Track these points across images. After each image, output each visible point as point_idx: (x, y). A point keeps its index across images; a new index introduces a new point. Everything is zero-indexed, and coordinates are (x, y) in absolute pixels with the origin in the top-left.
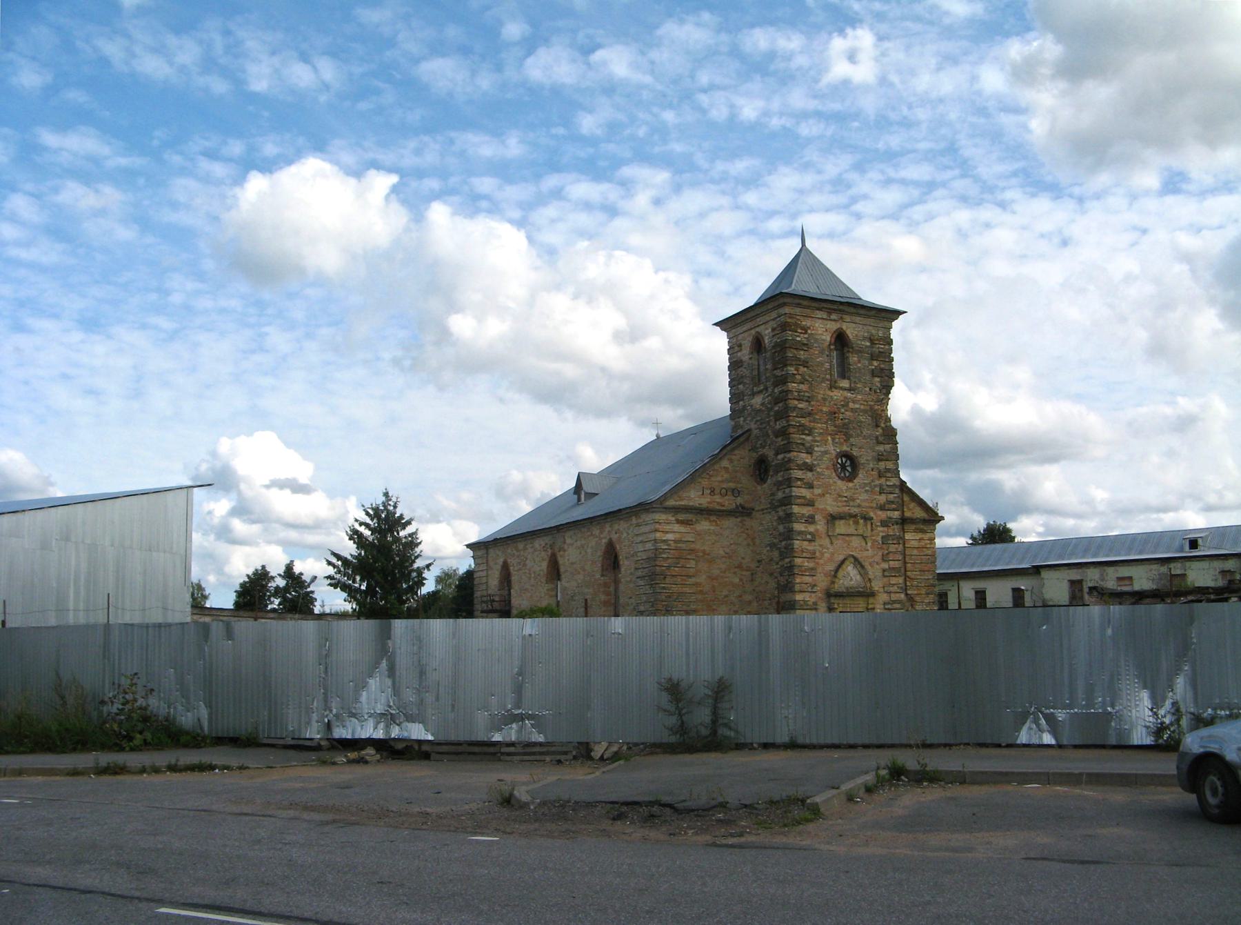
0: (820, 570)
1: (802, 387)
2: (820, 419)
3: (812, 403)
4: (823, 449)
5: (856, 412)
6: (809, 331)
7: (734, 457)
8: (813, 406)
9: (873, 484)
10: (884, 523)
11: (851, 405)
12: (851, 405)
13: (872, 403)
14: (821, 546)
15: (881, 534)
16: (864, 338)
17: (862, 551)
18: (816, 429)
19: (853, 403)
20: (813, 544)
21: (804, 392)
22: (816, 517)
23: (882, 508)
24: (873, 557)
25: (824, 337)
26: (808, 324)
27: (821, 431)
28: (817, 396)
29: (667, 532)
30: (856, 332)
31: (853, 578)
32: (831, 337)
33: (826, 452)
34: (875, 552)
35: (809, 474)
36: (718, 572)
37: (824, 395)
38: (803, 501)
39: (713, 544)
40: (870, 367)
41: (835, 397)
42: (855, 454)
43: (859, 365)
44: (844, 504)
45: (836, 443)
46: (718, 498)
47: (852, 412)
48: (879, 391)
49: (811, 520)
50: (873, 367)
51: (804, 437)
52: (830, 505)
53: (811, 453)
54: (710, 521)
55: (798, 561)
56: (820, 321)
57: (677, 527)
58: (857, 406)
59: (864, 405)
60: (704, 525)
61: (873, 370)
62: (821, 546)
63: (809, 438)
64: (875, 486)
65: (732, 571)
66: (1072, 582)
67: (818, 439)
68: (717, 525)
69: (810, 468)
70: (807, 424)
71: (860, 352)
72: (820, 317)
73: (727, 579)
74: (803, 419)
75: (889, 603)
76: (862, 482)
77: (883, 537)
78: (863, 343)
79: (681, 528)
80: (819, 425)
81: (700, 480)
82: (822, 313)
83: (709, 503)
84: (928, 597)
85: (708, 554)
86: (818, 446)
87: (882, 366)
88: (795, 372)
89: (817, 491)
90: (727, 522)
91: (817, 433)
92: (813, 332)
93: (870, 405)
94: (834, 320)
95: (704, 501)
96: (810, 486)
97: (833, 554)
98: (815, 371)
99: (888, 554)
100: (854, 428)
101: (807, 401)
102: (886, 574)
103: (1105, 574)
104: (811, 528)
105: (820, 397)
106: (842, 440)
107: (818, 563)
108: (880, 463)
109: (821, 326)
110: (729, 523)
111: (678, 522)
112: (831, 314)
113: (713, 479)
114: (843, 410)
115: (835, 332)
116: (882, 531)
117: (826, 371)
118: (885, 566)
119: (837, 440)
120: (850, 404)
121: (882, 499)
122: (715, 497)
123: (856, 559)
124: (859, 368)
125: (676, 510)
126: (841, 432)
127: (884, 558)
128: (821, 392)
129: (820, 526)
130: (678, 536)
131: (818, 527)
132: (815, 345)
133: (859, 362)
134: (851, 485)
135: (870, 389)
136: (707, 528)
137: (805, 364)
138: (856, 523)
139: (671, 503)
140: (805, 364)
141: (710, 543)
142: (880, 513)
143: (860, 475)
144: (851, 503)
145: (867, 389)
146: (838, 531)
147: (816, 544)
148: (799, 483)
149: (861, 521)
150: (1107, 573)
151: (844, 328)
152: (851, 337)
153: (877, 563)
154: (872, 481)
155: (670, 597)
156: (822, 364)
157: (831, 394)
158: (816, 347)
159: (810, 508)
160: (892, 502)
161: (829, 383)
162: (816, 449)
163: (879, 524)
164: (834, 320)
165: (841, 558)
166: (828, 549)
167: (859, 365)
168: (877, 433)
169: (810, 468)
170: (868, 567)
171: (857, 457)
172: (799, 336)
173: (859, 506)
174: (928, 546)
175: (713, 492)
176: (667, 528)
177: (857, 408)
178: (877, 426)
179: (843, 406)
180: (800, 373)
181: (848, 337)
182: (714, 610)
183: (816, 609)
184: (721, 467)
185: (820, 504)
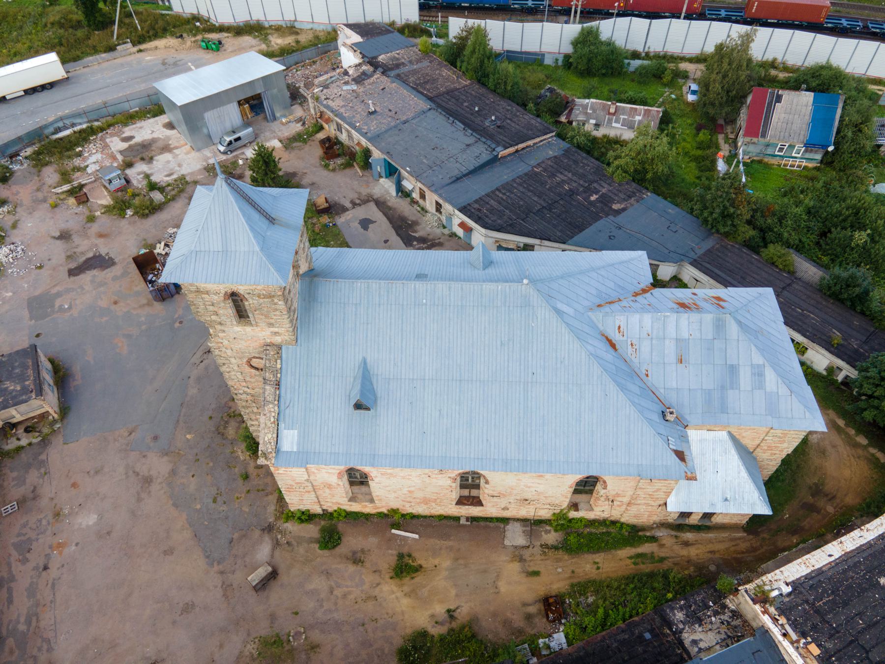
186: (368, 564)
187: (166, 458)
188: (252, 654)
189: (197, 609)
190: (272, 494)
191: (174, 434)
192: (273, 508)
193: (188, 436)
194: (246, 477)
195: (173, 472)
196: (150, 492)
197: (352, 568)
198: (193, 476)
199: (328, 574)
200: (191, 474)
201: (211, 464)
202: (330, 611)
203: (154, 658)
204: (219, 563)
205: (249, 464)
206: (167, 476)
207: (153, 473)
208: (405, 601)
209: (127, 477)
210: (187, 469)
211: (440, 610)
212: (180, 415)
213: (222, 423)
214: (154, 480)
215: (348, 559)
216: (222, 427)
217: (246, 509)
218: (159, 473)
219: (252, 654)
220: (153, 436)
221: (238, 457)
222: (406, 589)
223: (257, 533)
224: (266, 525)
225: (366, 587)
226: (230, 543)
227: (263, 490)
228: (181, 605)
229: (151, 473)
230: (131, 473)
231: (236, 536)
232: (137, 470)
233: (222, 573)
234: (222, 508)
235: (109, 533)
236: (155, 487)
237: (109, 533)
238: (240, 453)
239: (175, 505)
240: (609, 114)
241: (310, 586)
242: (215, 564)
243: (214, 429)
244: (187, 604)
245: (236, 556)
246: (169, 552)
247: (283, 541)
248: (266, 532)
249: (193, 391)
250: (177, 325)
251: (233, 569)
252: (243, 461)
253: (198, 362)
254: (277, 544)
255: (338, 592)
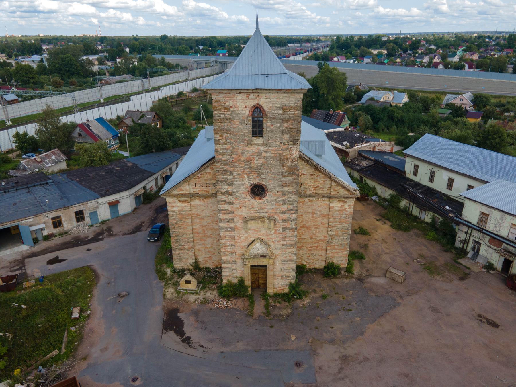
0: (238, 245)
1: (225, 146)
2: (239, 165)
3: (233, 156)
4: (240, 183)
5: (267, 158)
6: (232, 109)
7: (214, 167)
8: (233, 158)
9: (278, 200)
10: (284, 221)
11: (264, 154)
12: (264, 154)
13: (281, 152)
14: (238, 233)
15: (282, 227)
16: (278, 108)
17: (267, 235)
18: (236, 171)
19: (265, 152)
20: (233, 233)
21: (227, 149)
22: (235, 219)
23: (284, 213)
24: (274, 238)
25: (244, 112)
26: (231, 105)
27: (240, 172)
28: (237, 152)
29: (174, 207)
30: (271, 105)
31: (260, 249)
32: (250, 111)
33: (243, 184)
34: (277, 236)
35: (230, 197)
36: (206, 223)
37: (242, 150)
38: (226, 212)
39: (202, 211)
40: (281, 128)
41: (251, 151)
42: (265, 184)
43: (272, 128)
44: (256, 212)
45: (251, 179)
46: (204, 188)
47: (265, 159)
48: (286, 144)
49: (232, 220)
50: (284, 128)
51: (226, 177)
52: (245, 212)
53: (232, 186)
54: (200, 200)
55: (223, 241)
56: (241, 101)
57: (179, 204)
58: (268, 155)
59: (274, 153)
60: (196, 202)
61: (283, 130)
62: (238, 233)
63: (231, 177)
64: (279, 201)
65: (214, 223)
66: (483, 213)
67: (236, 177)
68: (205, 202)
69: (231, 194)
70: (229, 169)
71: (274, 118)
72: (241, 98)
73: (211, 227)
74: (225, 166)
75: (284, 261)
76: (270, 199)
77: (283, 228)
78: (276, 112)
79: (182, 204)
80: (238, 169)
81: (193, 180)
82: (241, 95)
83: (199, 191)
84: (343, 235)
85: (200, 216)
86: (236, 181)
87: (291, 126)
88: (221, 138)
89: (235, 206)
90: (210, 200)
91: (236, 174)
92: (234, 109)
93: (280, 154)
94: (252, 99)
95: (197, 190)
96: (231, 203)
97: (246, 238)
98: (236, 135)
99: (286, 237)
100: (265, 168)
101: (229, 155)
102: (283, 247)
103: (504, 218)
104: (232, 225)
105: (239, 151)
106: (255, 176)
107: (236, 242)
108: (284, 188)
109: (241, 104)
110: (210, 200)
111: (180, 201)
112: (249, 95)
113: (201, 179)
114: (257, 158)
115: (252, 107)
116: (282, 225)
117: (244, 134)
118: (285, 243)
119: (251, 177)
120: (263, 154)
121: (285, 207)
122: (203, 188)
123: (262, 240)
124: (272, 130)
125: (177, 196)
126: (255, 171)
127: (284, 238)
128: (240, 149)
129: (239, 223)
130: (180, 208)
131: (237, 224)
132: (236, 118)
133: (272, 125)
134: (261, 201)
135: (281, 143)
136: (199, 203)
137: (228, 131)
138: (263, 222)
139: (175, 192)
140: (228, 131)
141: (201, 210)
142: (282, 215)
143: (268, 196)
144: (261, 211)
145: (278, 143)
146: (249, 226)
147: (236, 233)
148: (223, 202)
149: (267, 221)
150: (506, 218)
151: (261, 103)
152: (266, 109)
153: (278, 241)
154: (277, 198)
155: (178, 235)
156: (241, 130)
157: (247, 148)
158: (237, 119)
159: (232, 215)
160: (292, 210)
161: (246, 142)
162: (235, 183)
163: (281, 221)
164: (252, 99)
165: (253, 239)
166: (244, 235)
167: (272, 128)
168: (284, 170)
169: (231, 194)
170: (272, 245)
171: (266, 186)
172: (223, 114)
173: (267, 212)
174: (348, 209)
175: (201, 185)
176: (174, 204)
177: (268, 156)
178: (283, 166)
179: (257, 156)
180: (224, 138)
181: (264, 109)
182: (204, 240)
183: (236, 264)
184: (206, 173)
185: (238, 213)
186: (366, 243)
187: (319, 351)
188: (441, 277)
189: (432, 305)
190: (335, 282)
191: (292, 350)
192: (345, 280)
193: (293, 338)
194: (324, 297)
195: (332, 342)
196: (356, 354)
197: (371, 247)
198: (332, 328)
199: (379, 255)
200: (330, 329)
201: (318, 318)
202: (399, 252)
203: (477, 321)
204: (396, 300)
205: (312, 297)
206: (336, 346)
207: (336, 356)
208: (380, 231)
209: (347, 377)
210: (326, 333)
211: (378, 223)
212: (270, 350)
213: (276, 318)
214: (344, 354)
215: (366, 249)
216: (281, 318)
217: (351, 292)
218: (335, 352)
219: (441, 277)
220: (295, 368)
221: (308, 303)
222: (373, 231)
223: (366, 285)
224: (359, 281)
225: (379, 243)
226: (379, 296)
227: (333, 286)
228: (434, 314)
229: (337, 358)
230: (341, 375)
231: (372, 294)
232: (336, 370)
233: (401, 297)
234: (355, 305)
235: (407, 375)
236: (350, 351)
237: (407, 375)
238: (305, 303)
239: (362, 333)
240: (39, 162)
241: (390, 261)
242: (397, 302)
243: (283, 323)
244: (432, 311)
245: (387, 292)
246: (402, 329)
247: (366, 273)
248: (364, 281)
249: (241, 346)
250: (137, 383)
251: (396, 292)
252: (311, 300)
253: (202, 349)
254: (370, 275)
255: (388, 251)
